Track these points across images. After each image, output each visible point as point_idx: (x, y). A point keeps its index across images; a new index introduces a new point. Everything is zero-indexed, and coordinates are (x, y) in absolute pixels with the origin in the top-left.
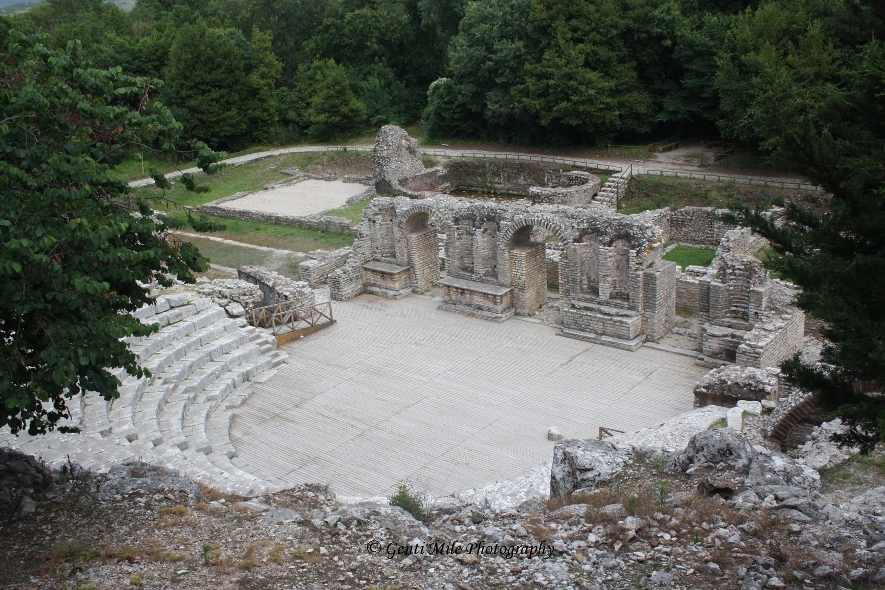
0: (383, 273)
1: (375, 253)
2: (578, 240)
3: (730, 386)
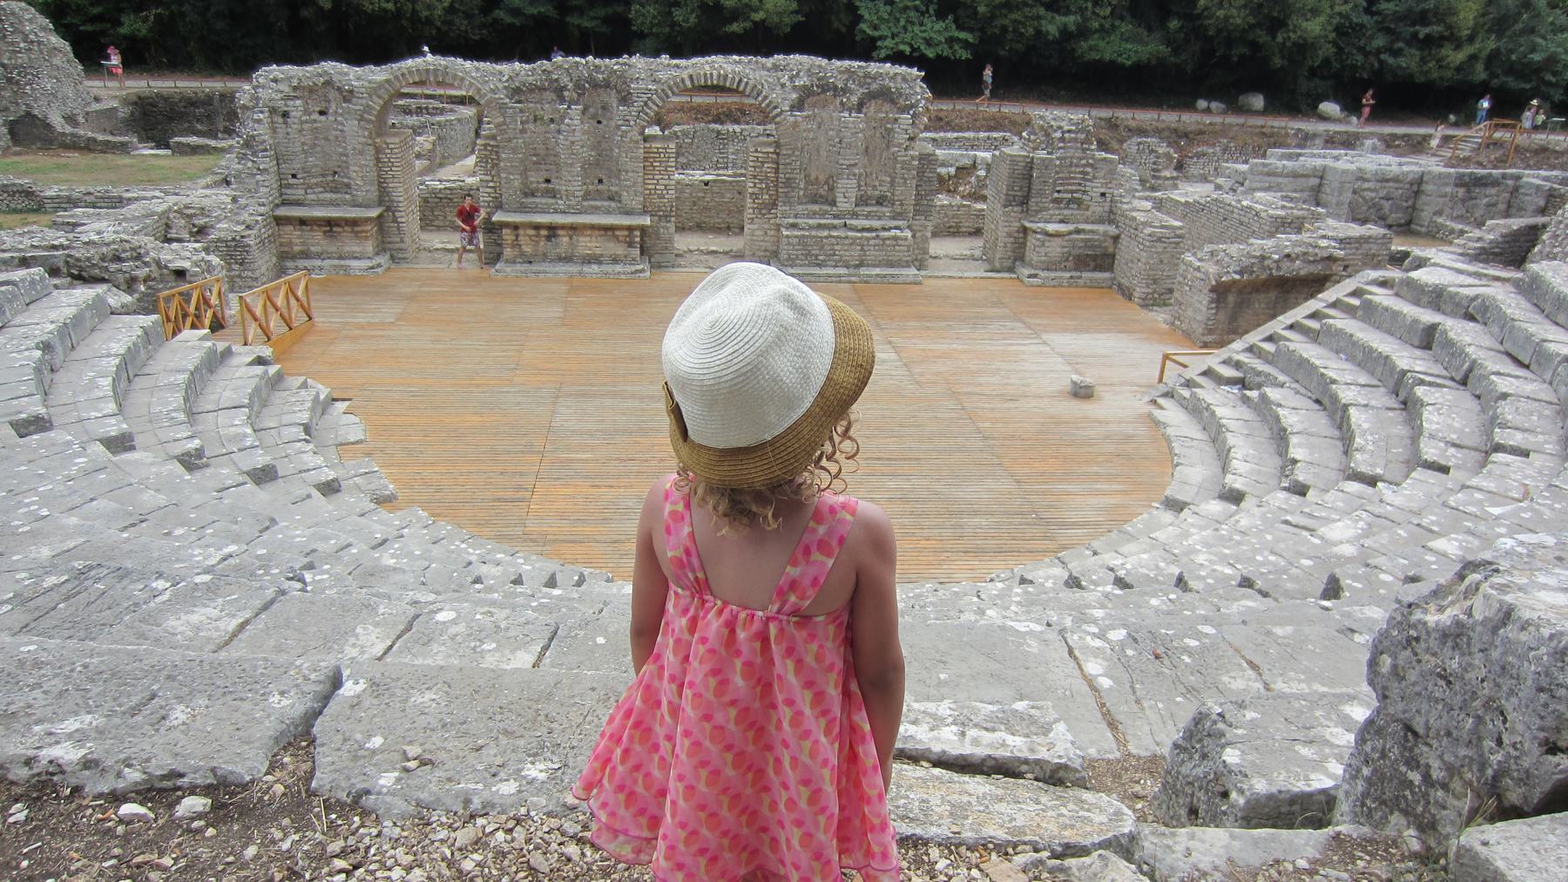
0: (330, 223)
1: (289, 186)
2: (798, 106)
3: (1277, 262)
